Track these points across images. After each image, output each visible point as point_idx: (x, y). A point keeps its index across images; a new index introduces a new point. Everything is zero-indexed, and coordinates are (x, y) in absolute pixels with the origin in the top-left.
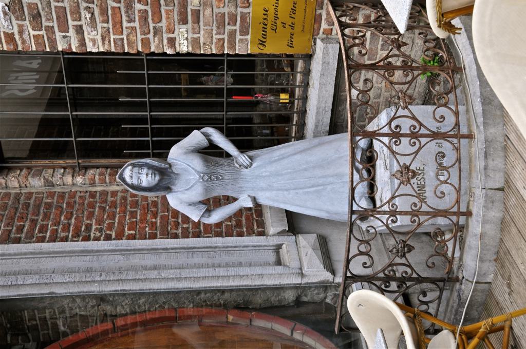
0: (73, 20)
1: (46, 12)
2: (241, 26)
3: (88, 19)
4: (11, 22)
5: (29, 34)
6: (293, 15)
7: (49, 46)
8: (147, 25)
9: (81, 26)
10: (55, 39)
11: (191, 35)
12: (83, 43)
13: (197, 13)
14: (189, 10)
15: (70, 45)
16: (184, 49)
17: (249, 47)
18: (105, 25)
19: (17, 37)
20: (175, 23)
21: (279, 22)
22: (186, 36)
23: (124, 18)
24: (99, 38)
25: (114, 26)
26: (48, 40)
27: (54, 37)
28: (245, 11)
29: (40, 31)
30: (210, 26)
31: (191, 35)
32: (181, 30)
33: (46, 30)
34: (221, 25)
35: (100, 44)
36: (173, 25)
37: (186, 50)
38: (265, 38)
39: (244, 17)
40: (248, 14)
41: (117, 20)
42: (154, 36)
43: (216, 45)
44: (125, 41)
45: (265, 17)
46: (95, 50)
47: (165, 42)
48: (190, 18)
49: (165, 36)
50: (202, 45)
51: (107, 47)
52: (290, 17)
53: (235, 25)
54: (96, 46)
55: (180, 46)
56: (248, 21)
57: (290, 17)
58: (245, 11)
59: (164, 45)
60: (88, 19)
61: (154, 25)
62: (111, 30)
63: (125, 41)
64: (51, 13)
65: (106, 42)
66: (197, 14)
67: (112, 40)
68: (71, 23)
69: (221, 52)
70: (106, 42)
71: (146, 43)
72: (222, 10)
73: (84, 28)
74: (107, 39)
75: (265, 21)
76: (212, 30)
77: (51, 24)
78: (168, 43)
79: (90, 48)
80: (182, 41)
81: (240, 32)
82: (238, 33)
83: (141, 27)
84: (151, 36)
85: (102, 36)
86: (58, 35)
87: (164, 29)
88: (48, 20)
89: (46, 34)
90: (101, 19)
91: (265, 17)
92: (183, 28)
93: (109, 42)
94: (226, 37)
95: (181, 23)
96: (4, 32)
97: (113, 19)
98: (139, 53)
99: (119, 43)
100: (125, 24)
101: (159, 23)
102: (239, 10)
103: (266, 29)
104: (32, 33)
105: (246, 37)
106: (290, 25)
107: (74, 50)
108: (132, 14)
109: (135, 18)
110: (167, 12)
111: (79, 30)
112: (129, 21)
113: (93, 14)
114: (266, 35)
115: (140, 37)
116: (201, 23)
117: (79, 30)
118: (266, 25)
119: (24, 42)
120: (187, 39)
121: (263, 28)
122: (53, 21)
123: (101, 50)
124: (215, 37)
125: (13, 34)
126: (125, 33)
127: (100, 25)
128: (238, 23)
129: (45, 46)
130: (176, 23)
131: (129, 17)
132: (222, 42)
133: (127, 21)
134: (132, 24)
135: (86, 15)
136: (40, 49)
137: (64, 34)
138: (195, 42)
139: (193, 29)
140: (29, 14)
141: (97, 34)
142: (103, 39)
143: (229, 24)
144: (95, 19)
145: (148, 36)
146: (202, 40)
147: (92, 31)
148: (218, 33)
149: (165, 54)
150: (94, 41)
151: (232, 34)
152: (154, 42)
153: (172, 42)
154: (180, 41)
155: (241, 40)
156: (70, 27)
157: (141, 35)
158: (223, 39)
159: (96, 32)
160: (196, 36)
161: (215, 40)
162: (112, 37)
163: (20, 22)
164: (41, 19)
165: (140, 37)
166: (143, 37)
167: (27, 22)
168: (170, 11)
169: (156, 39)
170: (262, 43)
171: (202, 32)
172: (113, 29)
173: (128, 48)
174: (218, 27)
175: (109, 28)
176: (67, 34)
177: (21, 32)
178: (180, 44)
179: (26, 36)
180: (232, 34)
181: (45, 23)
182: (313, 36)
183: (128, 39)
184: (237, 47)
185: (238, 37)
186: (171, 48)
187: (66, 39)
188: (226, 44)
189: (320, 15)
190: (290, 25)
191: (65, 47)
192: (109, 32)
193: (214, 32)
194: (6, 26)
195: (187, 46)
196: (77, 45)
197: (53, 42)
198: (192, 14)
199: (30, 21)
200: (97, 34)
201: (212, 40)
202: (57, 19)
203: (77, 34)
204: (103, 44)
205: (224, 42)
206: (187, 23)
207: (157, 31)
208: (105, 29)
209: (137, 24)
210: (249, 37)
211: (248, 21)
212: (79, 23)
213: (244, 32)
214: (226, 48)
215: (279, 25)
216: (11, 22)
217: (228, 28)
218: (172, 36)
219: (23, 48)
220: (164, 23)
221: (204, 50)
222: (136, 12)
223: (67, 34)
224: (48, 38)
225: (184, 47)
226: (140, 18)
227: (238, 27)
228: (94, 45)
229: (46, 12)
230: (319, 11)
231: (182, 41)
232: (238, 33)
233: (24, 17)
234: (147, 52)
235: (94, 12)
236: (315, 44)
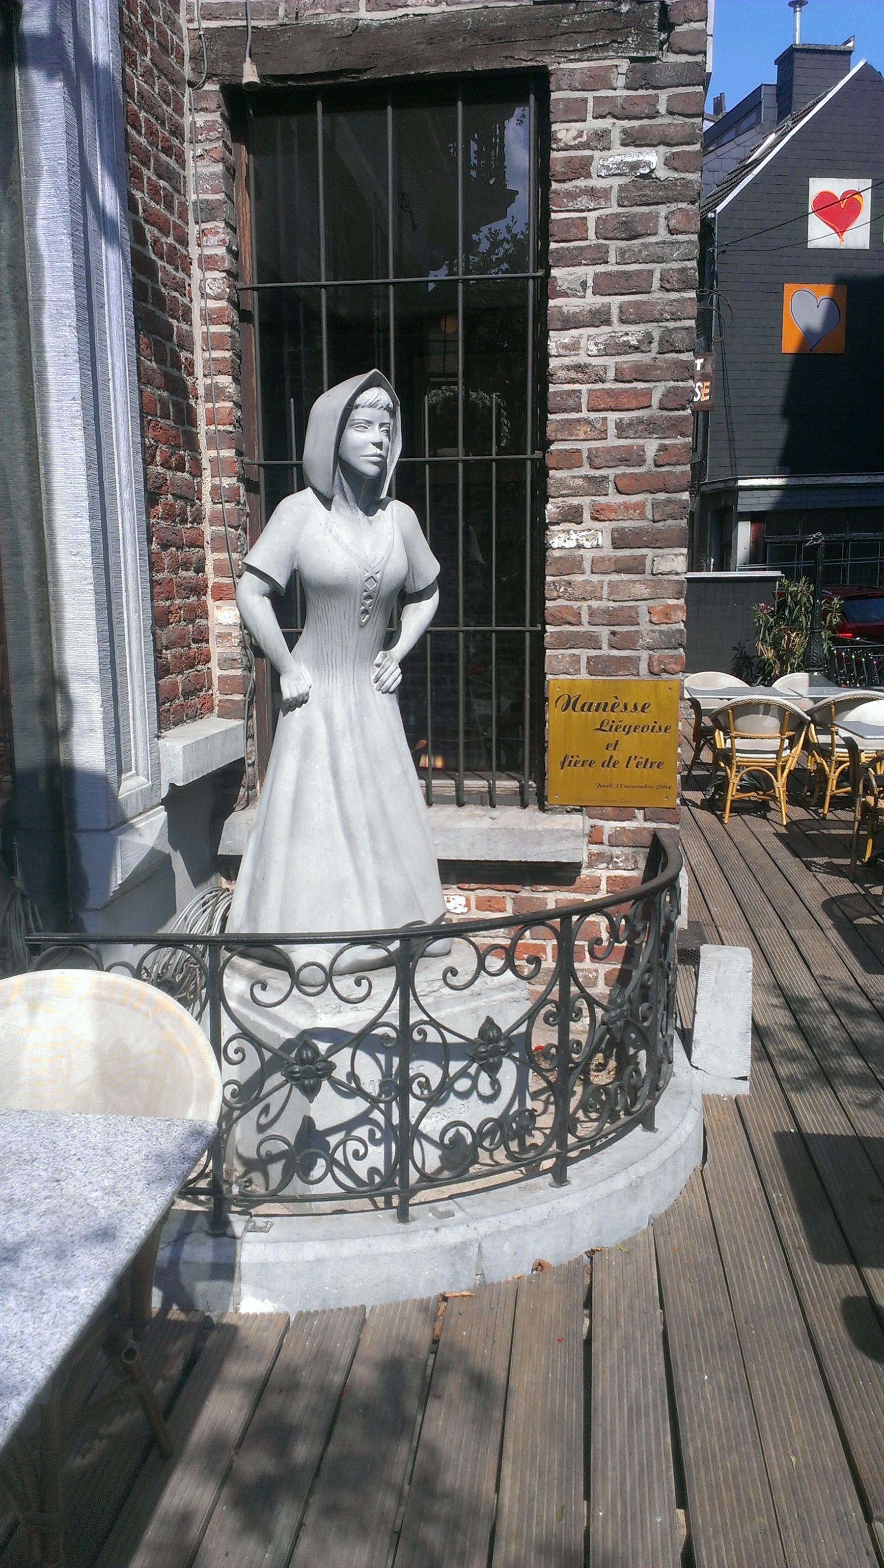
0: (620, 307)
1: (640, 251)
2: (610, 658)
3: (625, 338)
4: (614, 175)
5: (589, 210)
6: (633, 763)
7: (562, 248)
8: (611, 464)
9: (607, 322)
10: (580, 264)
11: (588, 555)
12: (569, 322)
13: (637, 568)
14: (644, 551)
15: (565, 295)
16: (556, 540)
17: (562, 677)
18: (611, 374)
19: (581, 183)
20: (614, 522)
21: (619, 735)
22: (587, 544)
23: (626, 416)
24: (583, 359)
25: (609, 392)
26: (575, 248)
27: (583, 262)
28: (643, 667)
29: (596, 233)
30: (610, 594)
31: (588, 555)
32: (600, 533)
33: (598, 246)
34: (611, 618)
35: (567, 361)
36: (612, 517)
37: (555, 546)
38: (582, 710)
39: (630, 664)
40: (635, 673)
41: (624, 401)
42: (585, 478)
43: (567, 607)
44: (574, 416)
45: (631, 707)
46: (553, 347)
47: (575, 501)
48: (627, 552)
49: (585, 501)
50: (566, 578)
51: (562, 374)
52: (630, 757)
53: (612, 647)
54: (562, 352)
55: (564, 531)
56: (621, 673)
57: (630, 757)
58: (643, 667)
59: (565, 499)
60: (625, 338)
61: (611, 478)
62: (599, 386)
63: (574, 416)
64: (636, 262)
65: (573, 375)
66: (635, 567)
67: (577, 387)
68: (615, 301)
69: (548, 619)
70: (573, 375)
71: (571, 459)
72: (644, 618)
73: (604, 329)
74: (580, 376)
75: (621, 707)
76: (601, 599)
77: (612, 258)
78: (571, 507)
79: (556, 340)
80: (574, 536)
81: (596, 656)
82: (593, 653)
83: (608, 450)
84: (586, 470)
85: (586, 366)
86: (588, 272)
87: (602, 500)
88: (622, 253)
89: (590, 246)
90: (624, 366)
91: (631, 707)
92: (604, 540)
93: (573, 381)
94: (585, 628)
95: (616, 535)
96: (591, 158)
97: (626, 391)
98: (544, 444)
99: (571, 402)
100: (613, 417)
101: (617, 488)
102: (645, 655)
103: (604, 710)
104: (592, 216)
105: (583, 670)
106: (611, 757)
107: (551, 303)
108: (636, 432)
109: (626, 438)
110: (641, 506)
111: (600, 318)
112: (619, 426)
113: (636, 349)
114: (589, 710)
115: (584, 446)
116: (615, 577)
117: (600, 318)
118: (612, 710)
119: (571, 195)
120: (580, 547)
121: (607, 704)
122: (617, 263)
123: (553, 363)
124: (585, 604)
125: (589, 176)
126: (593, 416)
127: (610, 362)
128: (615, 653)
129: (563, 241)
130: (614, 524)
131: (630, 425)
132: (572, 620)
133: (621, 420)
134: (612, 431)
135: (634, 333)
136: (553, 229)
137: (590, 283)
138: (572, 564)
139: (602, 559)
140: (635, 215)
141: (589, 355)
142: (579, 368)
143: (613, 633)
144: (626, 353)
145: (586, 466)
146: (578, 578)
147: (596, 344)
148: (592, 613)
149: (545, 499)
150: (573, 347)
151: (592, 642)
152: (574, 477)
153: (574, 516)
154: (575, 532)
155: (576, 659)
156: (607, 299)
157: (589, 450)
158: (580, 624)
159: (595, 352)
160: (587, 565)
161: (576, 605)
162: (584, 388)
163: (614, 194)
164: (622, 239)
165: (584, 446)
166: (585, 455)
167: (615, 209)
168: (643, 512)
169: (580, 482)
170: (570, 704)
171: (595, 578)
172: (604, 389)
173: (558, 421)
174: (606, 611)
175: (603, 381)
176: (589, 291)
177: (592, 192)
178: (568, 532)
179: (584, 201)
180: (592, 642)
181: (613, 246)
182: (586, 807)
183: (578, 421)
184: (562, 651)
185: (584, 654)
186: (559, 513)
187: (580, 288)
188: (567, 628)
189: (632, 818)
190: (611, 757)
191: (560, 282)
192: (596, 382)
193: (595, 604)
194: (606, 164)
195: (563, 548)
196: (565, 309)
197: (573, 259)
198: (635, 558)
199: (618, 215)
200: (589, 355)
201: (576, 600)
202: (625, 273)
203: (590, 311)
204: (568, 368)
205: (570, 624)
206: (614, 548)
207: (596, 485)
208: (602, 373)
209: (612, 441)
210: (584, 675)
211: (621, 673)
212: (615, 318)
213: (596, 666)
214: (558, 629)
215: (612, 737)
216: (614, 175)
217: (604, 632)
218: (586, 516)
219: (556, 192)
220: (614, 498)
221: (554, 583)
222: (640, 441)
223: (589, 291)
224: (582, 249)
225: (561, 540)
226: (629, 448)
227: (606, 651)
228: (565, 347)
229: (640, 251)
230: (640, 814)
231: (574, 536)
232: (593, 653)
233: (626, 203)
234: (549, 461)
235: (642, 351)
236: (568, 812)
